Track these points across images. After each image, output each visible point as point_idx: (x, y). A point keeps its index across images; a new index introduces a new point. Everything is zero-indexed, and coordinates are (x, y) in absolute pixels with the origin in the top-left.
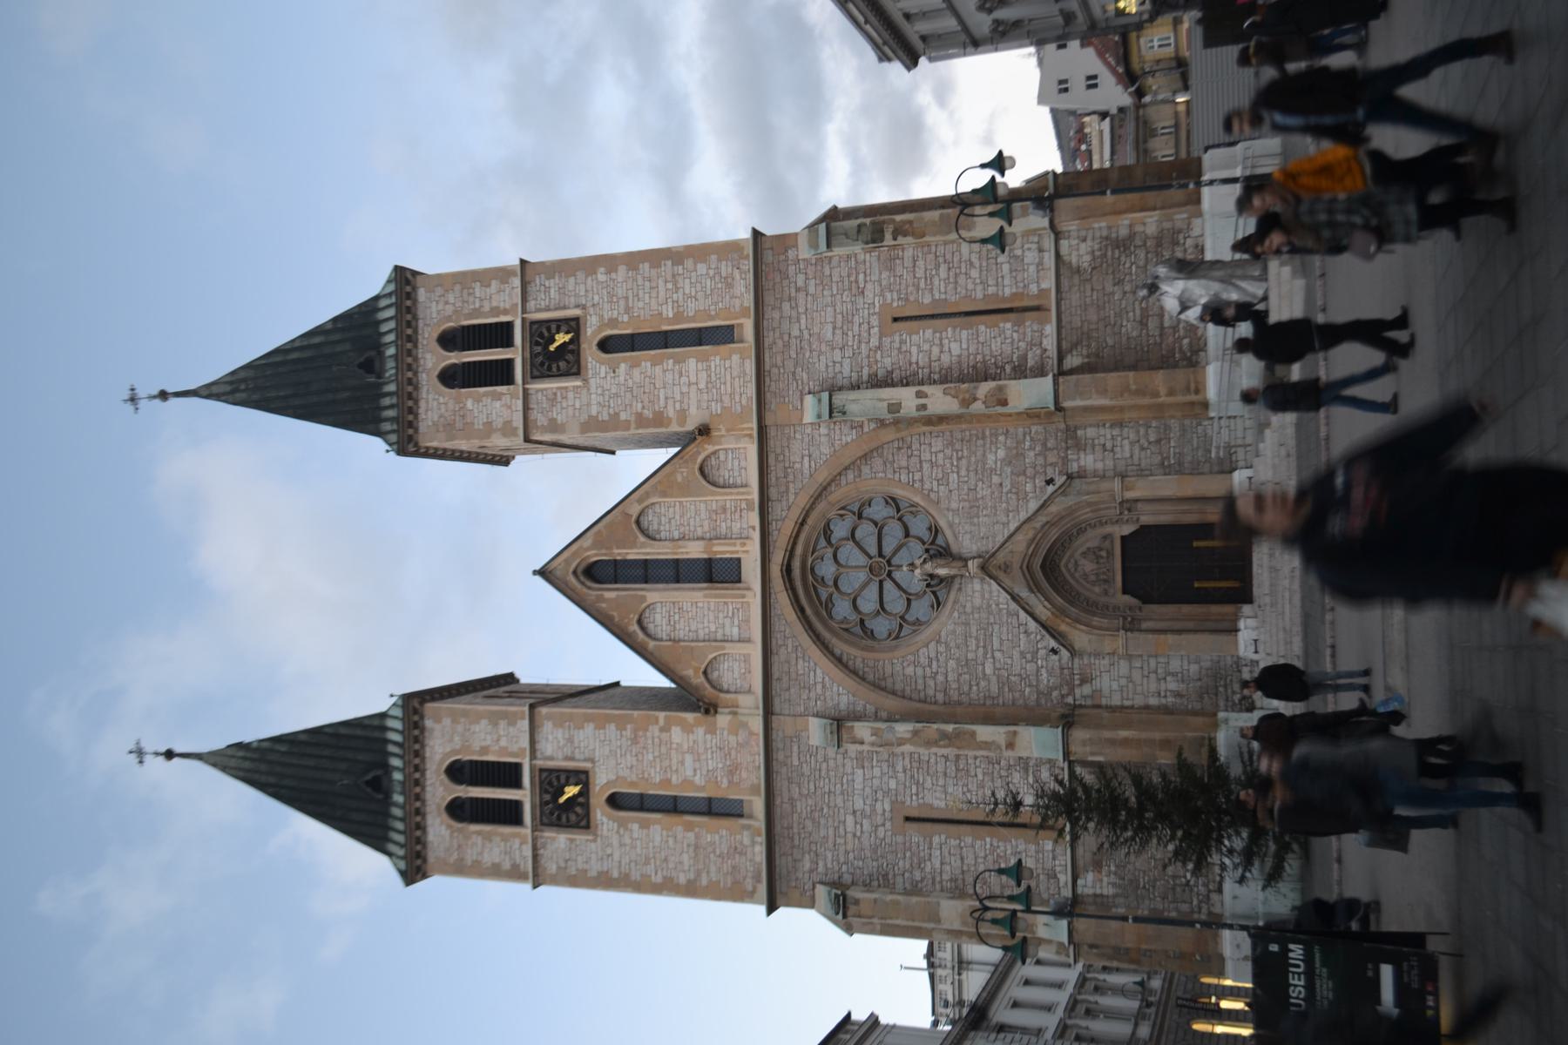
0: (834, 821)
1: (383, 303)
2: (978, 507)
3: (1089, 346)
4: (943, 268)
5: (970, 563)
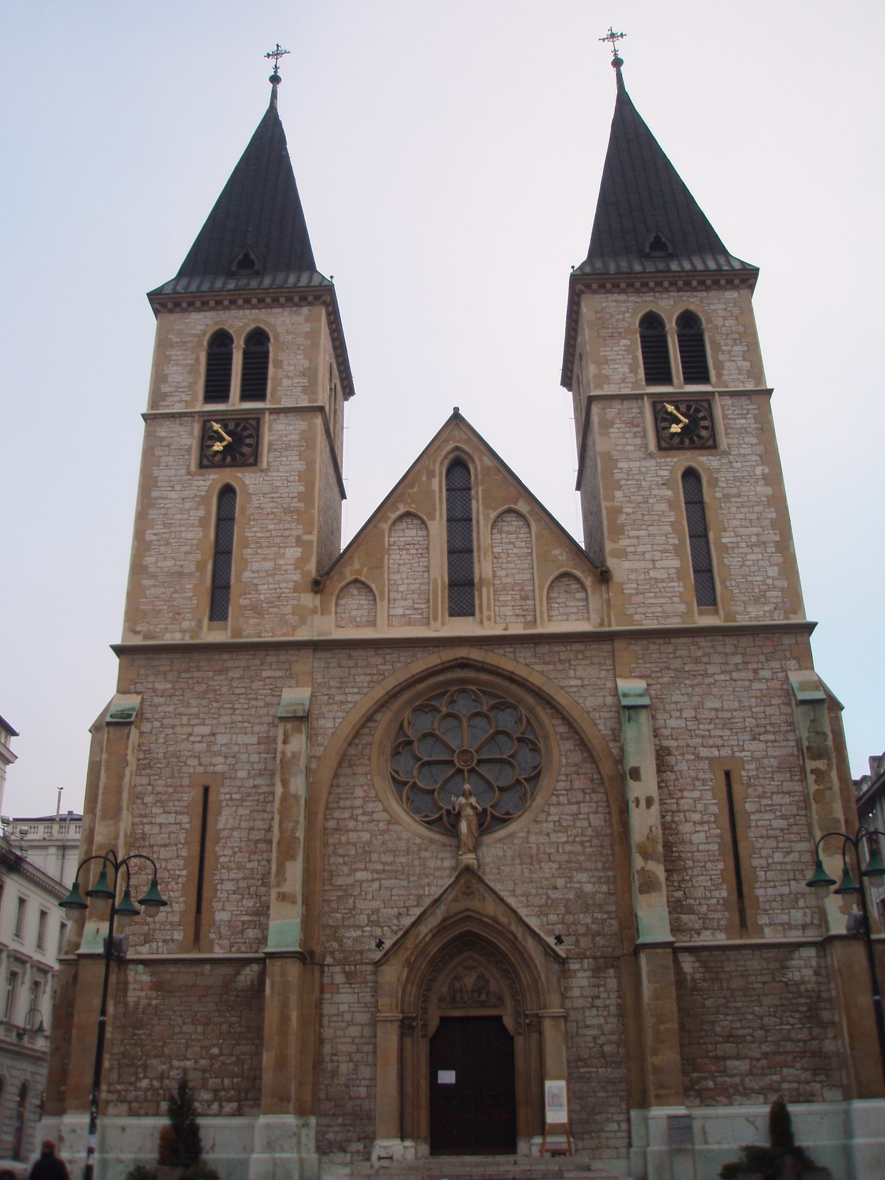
0: (205, 713)
1: (722, 260)
2: (531, 864)
4: (783, 823)
5: (472, 855)
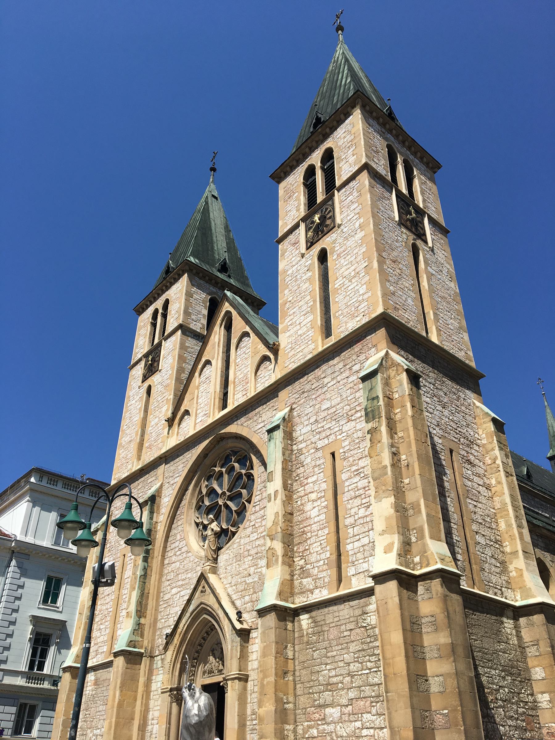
3: (314, 634)
4: (364, 483)
